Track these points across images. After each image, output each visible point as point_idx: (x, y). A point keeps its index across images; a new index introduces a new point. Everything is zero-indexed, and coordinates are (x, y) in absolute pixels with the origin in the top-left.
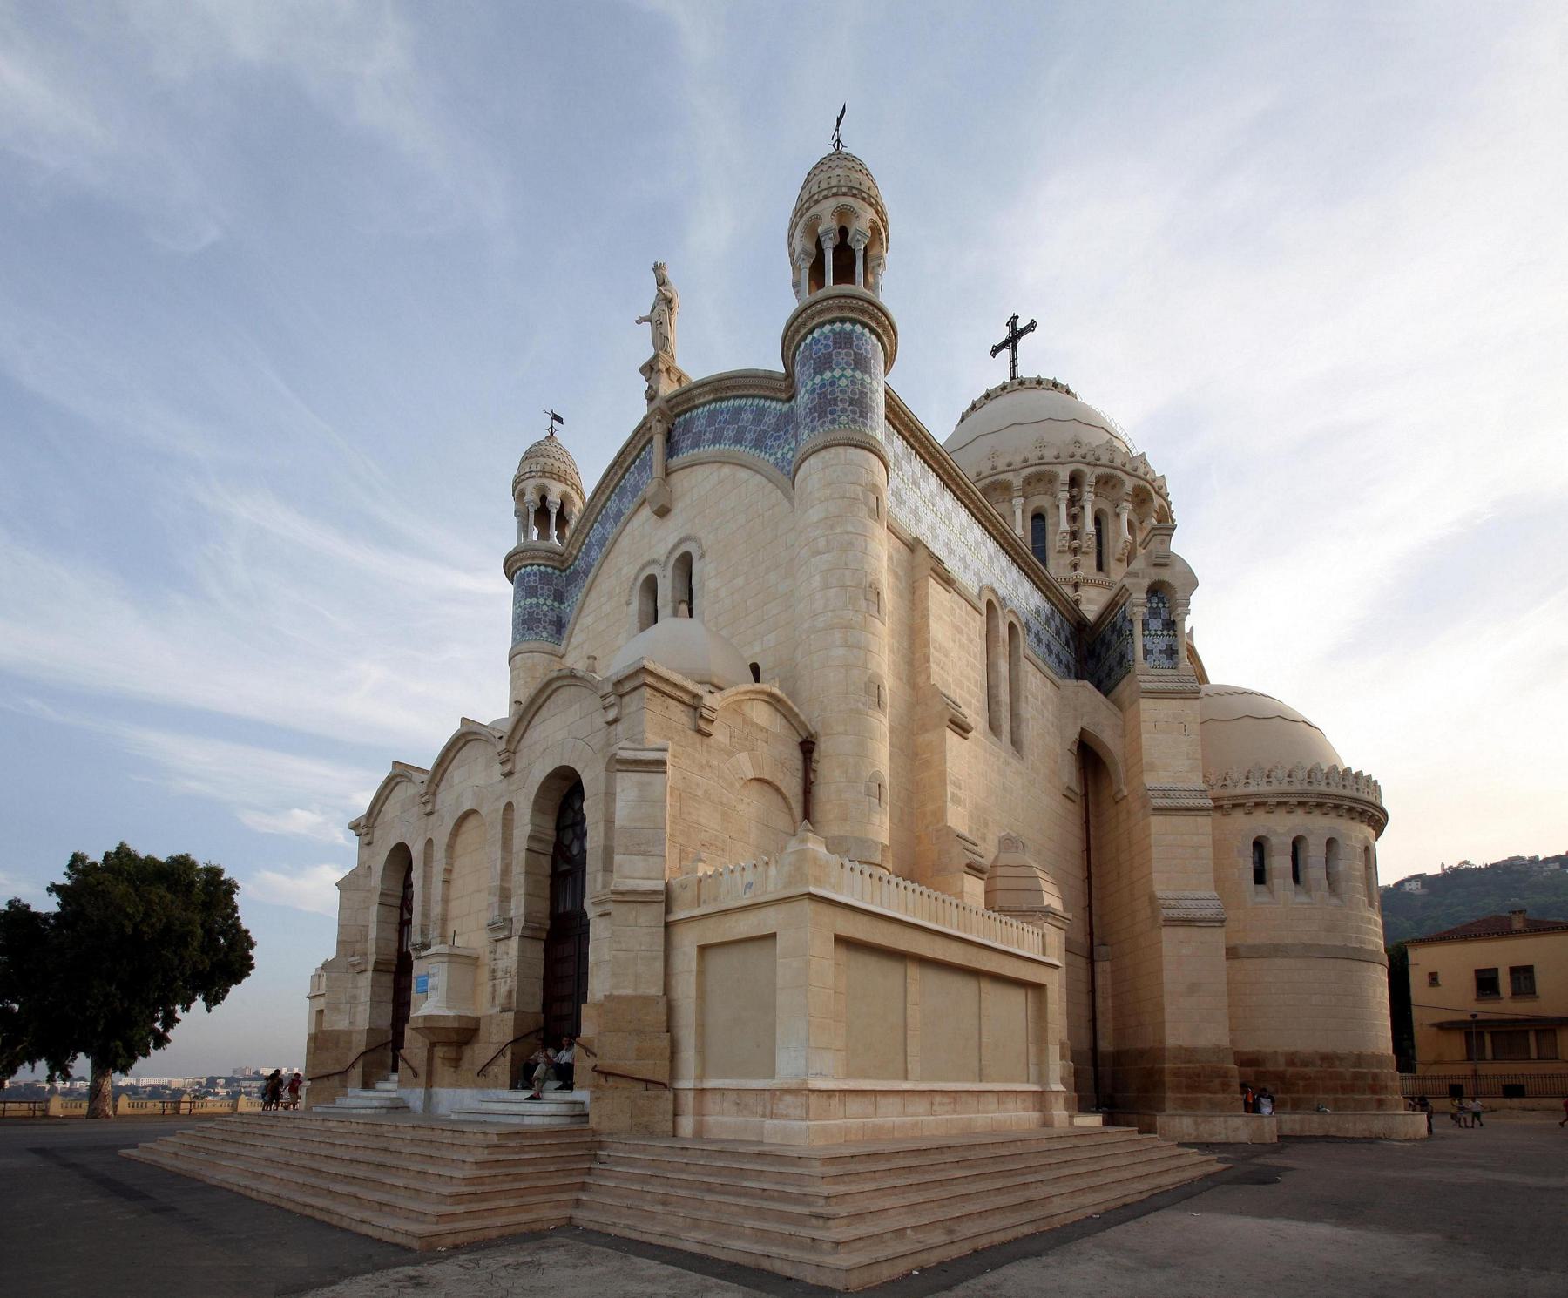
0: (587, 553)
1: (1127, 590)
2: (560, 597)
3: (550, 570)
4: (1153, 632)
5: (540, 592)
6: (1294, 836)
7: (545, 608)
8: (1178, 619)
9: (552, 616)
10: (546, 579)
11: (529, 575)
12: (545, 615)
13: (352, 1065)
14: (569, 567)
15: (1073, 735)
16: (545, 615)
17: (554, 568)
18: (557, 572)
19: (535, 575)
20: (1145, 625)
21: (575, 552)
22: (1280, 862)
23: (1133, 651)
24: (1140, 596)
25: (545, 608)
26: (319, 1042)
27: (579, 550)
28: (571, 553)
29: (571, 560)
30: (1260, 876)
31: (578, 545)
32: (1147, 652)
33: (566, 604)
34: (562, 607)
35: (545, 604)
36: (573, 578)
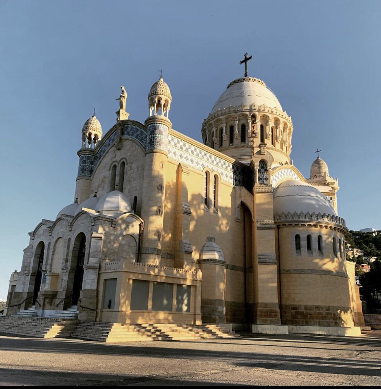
0: (100, 153)
2: (92, 163)
3: (90, 156)
5: (87, 162)
6: (307, 235)
9: (89, 169)
10: (88, 158)
13: (22, 303)
15: (238, 202)
16: (87, 168)
17: (91, 155)
18: (92, 156)
20: (259, 171)
21: (97, 152)
22: (304, 243)
25: (88, 167)
26: (12, 295)
28: (96, 152)
29: (96, 154)
30: (298, 247)
31: (98, 150)
36: (96, 158)
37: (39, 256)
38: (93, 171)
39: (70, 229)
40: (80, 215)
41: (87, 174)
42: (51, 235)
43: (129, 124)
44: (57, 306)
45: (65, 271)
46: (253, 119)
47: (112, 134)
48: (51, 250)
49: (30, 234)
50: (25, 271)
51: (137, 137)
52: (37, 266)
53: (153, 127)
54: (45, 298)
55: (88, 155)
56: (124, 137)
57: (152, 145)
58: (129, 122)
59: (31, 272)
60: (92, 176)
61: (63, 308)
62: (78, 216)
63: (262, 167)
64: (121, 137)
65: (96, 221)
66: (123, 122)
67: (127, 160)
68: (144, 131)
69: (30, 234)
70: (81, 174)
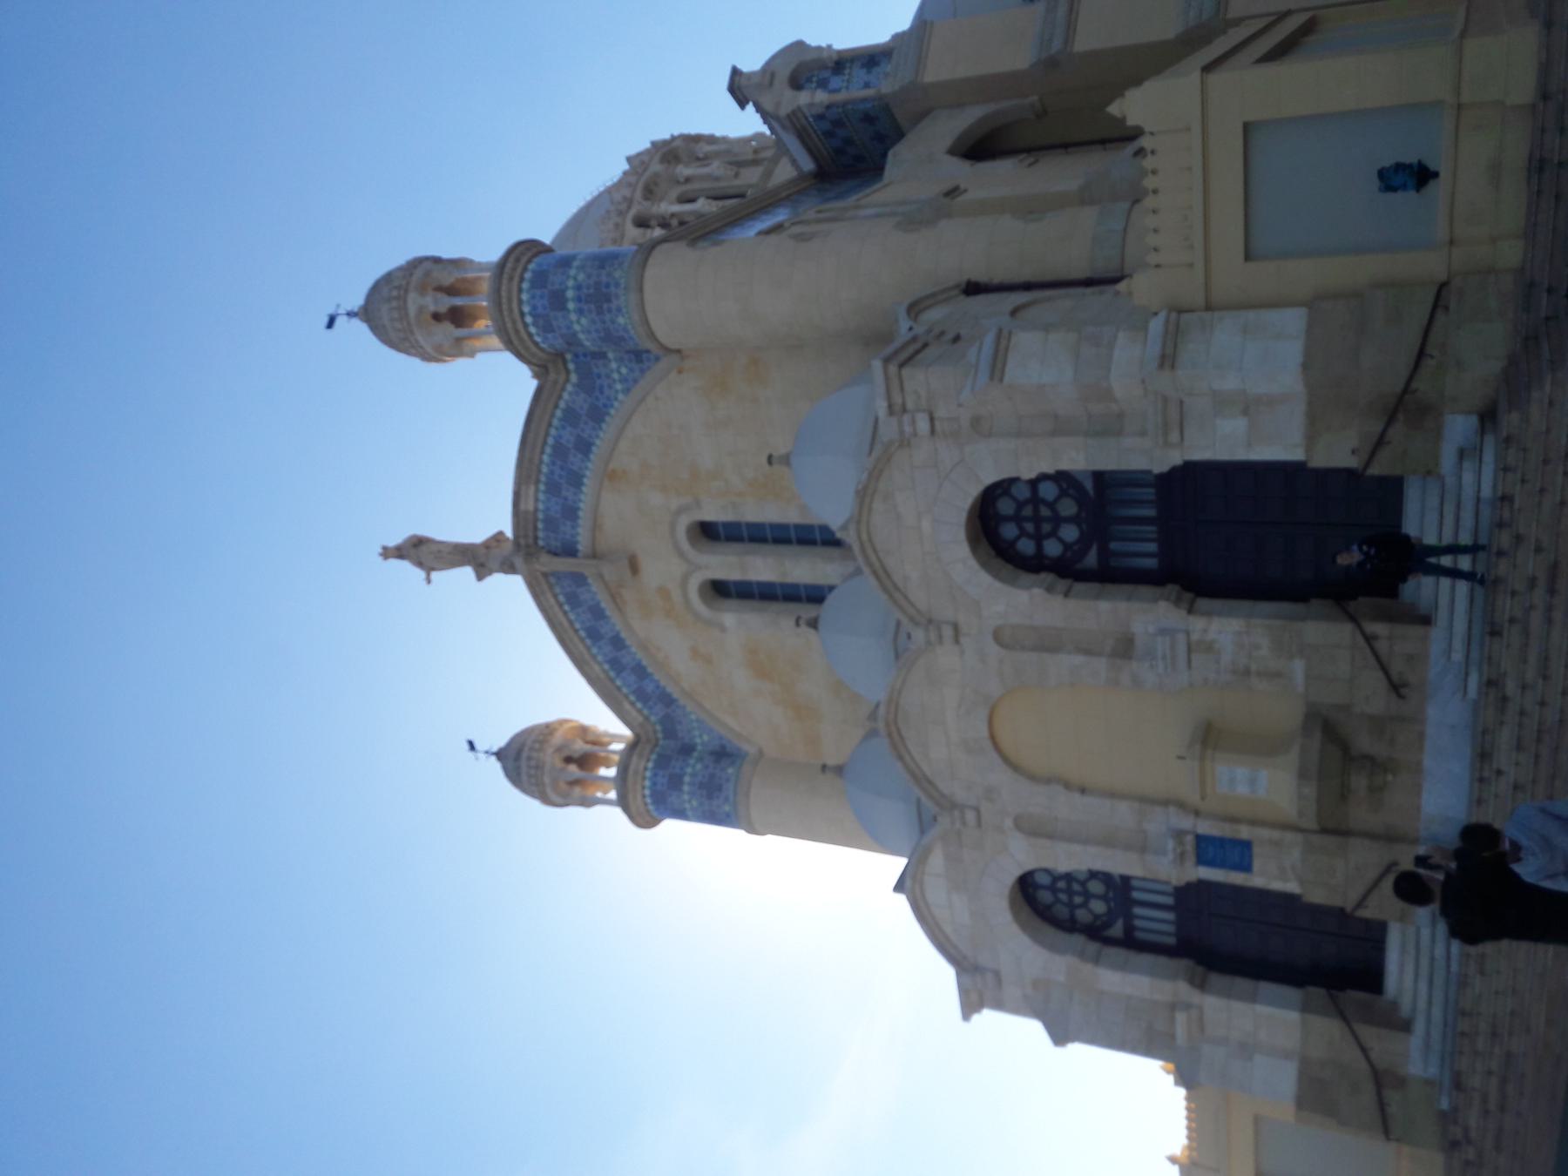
1: (794, 112)
2: (687, 750)
3: (654, 757)
4: (845, 84)
7: (699, 766)
8: (835, 57)
10: (663, 762)
11: (654, 784)
12: (707, 767)
14: (655, 732)
19: (655, 775)
23: (864, 100)
24: (804, 98)
27: (640, 711)
31: (634, 713)
32: (867, 85)
33: (698, 740)
34: (699, 748)
35: (694, 766)
36: (669, 727)
37: (1093, 947)
38: (723, 747)
39: (948, 632)
40: (873, 558)
41: (730, 771)
42: (977, 810)
43: (531, 507)
44: (1397, 688)
45: (1181, 638)
46: (653, 223)
47: (571, 623)
48: (1065, 807)
49: (970, 1006)
50: (1173, 1037)
51: (585, 447)
52: (1146, 959)
53: (533, 297)
54: (1345, 833)
55: (650, 765)
56: (583, 543)
57: (613, 289)
58: (522, 507)
59: (1183, 989)
60: (745, 747)
61: (1415, 631)
62: (881, 572)
63: (823, 84)
64: (587, 557)
65: (910, 405)
66: (522, 542)
67: (680, 511)
68: (562, 404)
69: (970, 1006)
70: (727, 799)
